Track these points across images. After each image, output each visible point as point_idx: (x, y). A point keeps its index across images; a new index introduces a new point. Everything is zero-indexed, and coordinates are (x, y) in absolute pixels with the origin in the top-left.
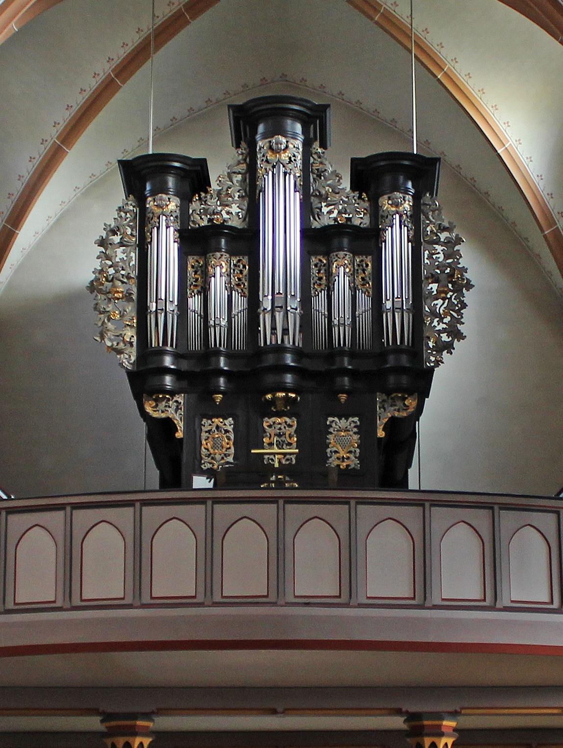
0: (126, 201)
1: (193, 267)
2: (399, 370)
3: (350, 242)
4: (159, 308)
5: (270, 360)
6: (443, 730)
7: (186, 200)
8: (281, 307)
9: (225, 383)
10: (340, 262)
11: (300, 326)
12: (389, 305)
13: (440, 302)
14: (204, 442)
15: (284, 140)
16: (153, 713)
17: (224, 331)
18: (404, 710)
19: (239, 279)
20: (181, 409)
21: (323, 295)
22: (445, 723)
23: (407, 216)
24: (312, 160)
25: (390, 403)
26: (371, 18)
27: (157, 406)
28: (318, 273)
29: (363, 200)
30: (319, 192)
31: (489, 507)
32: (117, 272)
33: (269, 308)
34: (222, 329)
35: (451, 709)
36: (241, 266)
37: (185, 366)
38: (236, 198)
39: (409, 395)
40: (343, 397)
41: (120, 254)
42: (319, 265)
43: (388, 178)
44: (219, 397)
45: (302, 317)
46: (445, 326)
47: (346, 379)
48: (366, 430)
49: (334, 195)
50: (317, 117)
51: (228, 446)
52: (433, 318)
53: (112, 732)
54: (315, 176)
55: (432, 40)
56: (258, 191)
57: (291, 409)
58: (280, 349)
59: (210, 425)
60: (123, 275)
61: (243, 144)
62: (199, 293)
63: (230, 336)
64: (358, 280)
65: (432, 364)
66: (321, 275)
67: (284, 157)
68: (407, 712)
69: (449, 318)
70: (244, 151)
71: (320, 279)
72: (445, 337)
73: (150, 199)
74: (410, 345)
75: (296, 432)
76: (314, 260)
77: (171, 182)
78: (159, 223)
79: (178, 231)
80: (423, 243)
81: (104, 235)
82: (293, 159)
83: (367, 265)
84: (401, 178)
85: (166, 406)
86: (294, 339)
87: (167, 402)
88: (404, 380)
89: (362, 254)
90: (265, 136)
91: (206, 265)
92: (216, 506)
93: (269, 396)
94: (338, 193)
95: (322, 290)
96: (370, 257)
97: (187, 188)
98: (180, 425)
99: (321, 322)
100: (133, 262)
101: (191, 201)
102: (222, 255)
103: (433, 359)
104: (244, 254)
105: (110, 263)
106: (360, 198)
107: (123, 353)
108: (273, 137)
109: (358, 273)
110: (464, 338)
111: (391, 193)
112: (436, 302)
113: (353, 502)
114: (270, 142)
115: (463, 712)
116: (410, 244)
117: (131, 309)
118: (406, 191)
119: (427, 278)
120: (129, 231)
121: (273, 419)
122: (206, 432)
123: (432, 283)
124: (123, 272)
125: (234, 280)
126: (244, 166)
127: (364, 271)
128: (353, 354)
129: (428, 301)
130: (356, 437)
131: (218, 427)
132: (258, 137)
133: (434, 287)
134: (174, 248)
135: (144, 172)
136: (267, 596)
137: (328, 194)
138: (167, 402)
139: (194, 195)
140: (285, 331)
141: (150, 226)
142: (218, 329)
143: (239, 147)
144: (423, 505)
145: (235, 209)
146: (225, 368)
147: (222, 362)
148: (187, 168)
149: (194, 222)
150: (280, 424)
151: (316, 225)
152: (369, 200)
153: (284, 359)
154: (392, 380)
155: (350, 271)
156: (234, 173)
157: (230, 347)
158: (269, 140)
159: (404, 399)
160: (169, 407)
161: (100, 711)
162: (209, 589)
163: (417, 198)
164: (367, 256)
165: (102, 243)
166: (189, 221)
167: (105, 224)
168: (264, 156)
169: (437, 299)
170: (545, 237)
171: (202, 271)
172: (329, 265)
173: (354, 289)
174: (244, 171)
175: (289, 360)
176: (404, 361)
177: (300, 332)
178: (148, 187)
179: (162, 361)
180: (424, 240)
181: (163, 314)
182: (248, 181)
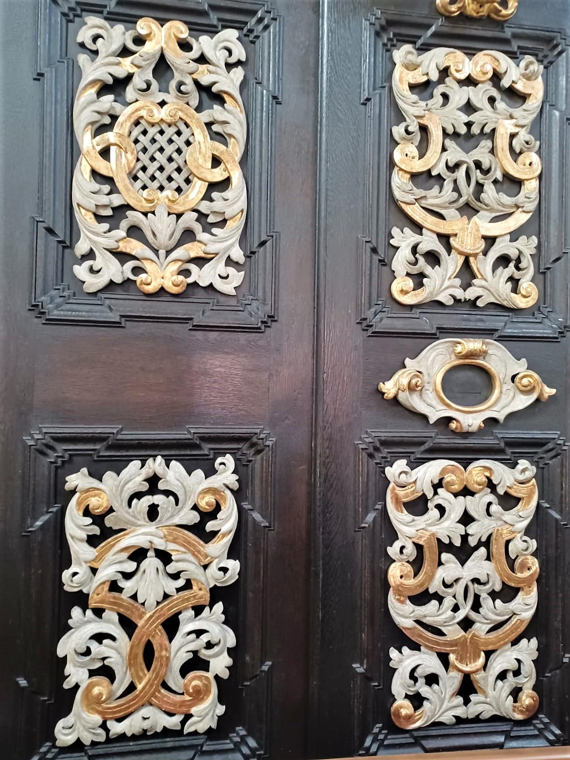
14: (88, 143)
51: (218, 175)
59: (125, 52)
75: (537, 127)
121: (438, 57)
122: (104, 89)
131: (162, 67)
150: (470, 81)
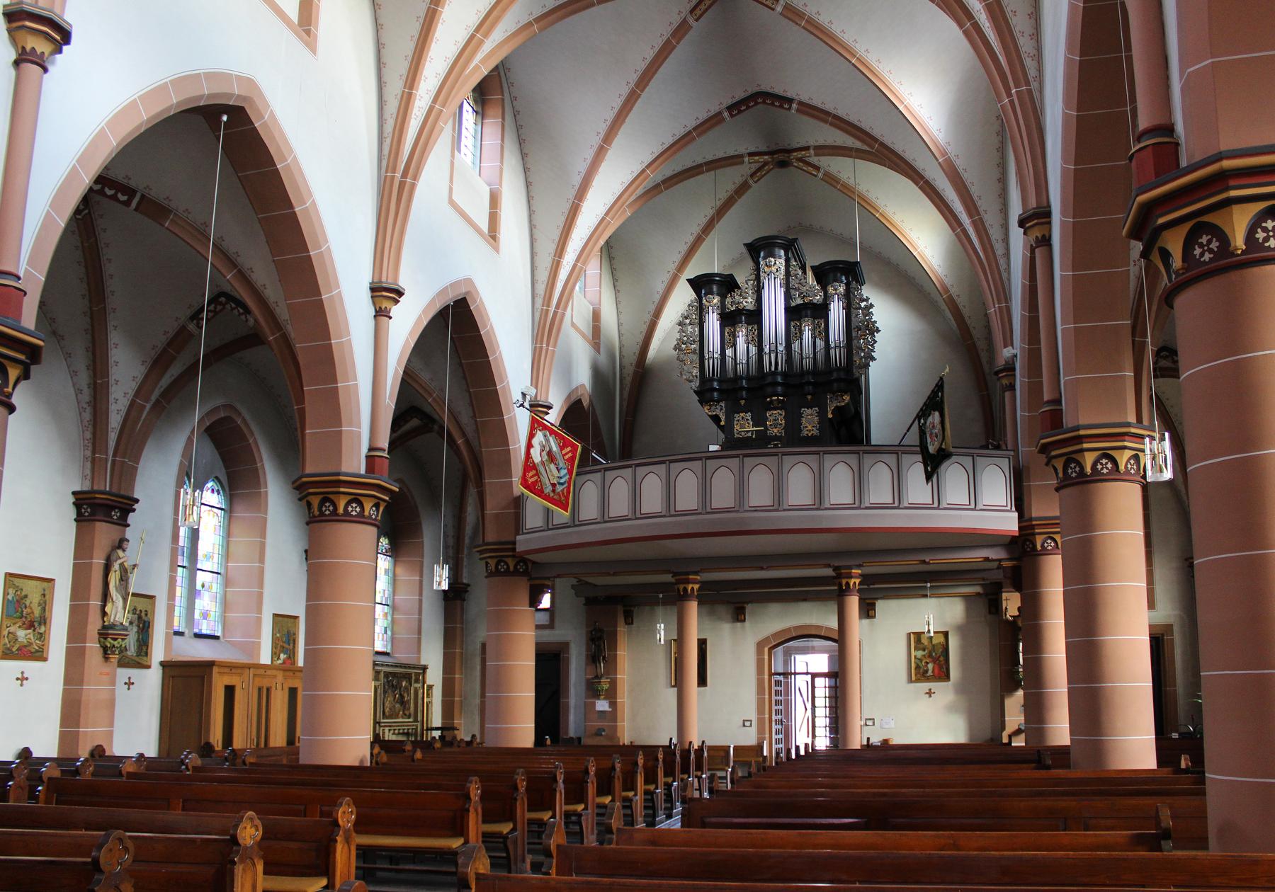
5: (769, 379)
7: (723, 297)
9: (746, 394)
15: (773, 260)
17: (745, 366)
21: (798, 342)
24: (791, 269)
37: (725, 386)
38: (750, 294)
40: (809, 397)
41: (690, 329)
44: (743, 402)
48: (822, 414)
53: (679, 582)
57: (782, 406)
58: (775, 373)
62: (732, 346)
64: (817, 333)
67: (774, 269)
76: (792, 324)
77: (715, 288)
81: (681, 319)
93: (768, 399)
98: (723, 418)
101: (726, 298)
117: (696, 357)
120: (694, 317)
125: (750, 338)
130: (817, 418)
134: (717, 324)
145: (750, 300)
148: (723, 280)
149: (728, 309)
151: (793, 304)
173: (814, 338)
175: (779, 379)
179: (712, 385)
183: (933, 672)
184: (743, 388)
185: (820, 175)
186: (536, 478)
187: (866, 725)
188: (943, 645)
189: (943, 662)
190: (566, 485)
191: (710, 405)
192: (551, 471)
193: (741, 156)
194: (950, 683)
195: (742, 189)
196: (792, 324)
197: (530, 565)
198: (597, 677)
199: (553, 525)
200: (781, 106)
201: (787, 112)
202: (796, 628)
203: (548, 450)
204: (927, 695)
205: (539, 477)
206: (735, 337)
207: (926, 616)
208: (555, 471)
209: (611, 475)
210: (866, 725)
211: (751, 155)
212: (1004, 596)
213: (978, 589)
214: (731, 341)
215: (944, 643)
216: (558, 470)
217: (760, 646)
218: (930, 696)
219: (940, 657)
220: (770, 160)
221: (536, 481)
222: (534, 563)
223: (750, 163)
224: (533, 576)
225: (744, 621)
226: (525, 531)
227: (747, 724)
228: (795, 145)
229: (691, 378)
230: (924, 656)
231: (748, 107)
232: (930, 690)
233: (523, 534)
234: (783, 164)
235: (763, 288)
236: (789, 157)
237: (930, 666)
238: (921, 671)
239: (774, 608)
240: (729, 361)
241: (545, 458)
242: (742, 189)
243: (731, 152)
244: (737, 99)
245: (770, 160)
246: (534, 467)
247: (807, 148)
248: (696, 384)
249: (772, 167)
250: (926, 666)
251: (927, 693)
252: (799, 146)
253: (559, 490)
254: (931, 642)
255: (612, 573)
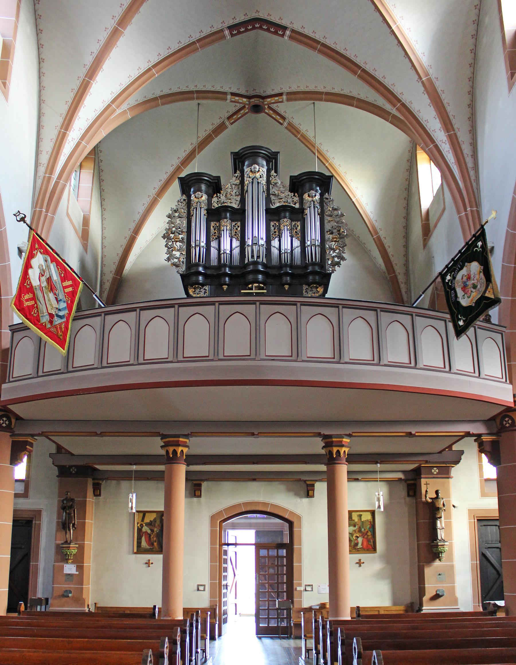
0: (181, 197)
1: (213, 227)
2: (314, 273)
3: (290, 215)
4: (196, 245)
5: (251, 267)
6: (343, 443)
7: (210, 197)
8: (257, 243)
10: (285, 224)
11: (266, 255)
12: (309, 243)
13: (334, 243)
15: (258, 167)
16: (188, 434)
17: (228, 256)
18: (322, 433)
19: (236, 232)
20: (207, 292)
21: (277, 240)
22: (344, 440)
23: (317, 202)
24: (271, 179)
25: (310, 290)
26: (296, 136)
27: (195, 291)
28: (274, 230)
29: (295, 196)
30: (274, 192)
31: (375, 309)
32: (176, 229)
33: (250, 244)
34: (228, 255)
35: (348, 433)
36: (237, 227)
37: (209, 272)
39: (320, 286)
41: (178, 221)
42: (274, 226)
43: (307, 186)
44: (225, 287)
45: (266, 249)
46: (336, 254)
47: (288, 278)
49: (282, 194)
50: (274, 158)
52: (330, 250)
54: (272, 186)
55: (324, 148)
56: (245, 192)
58: (256, 263)
60: (179, 231)
61: (238, 172)
62: (216, 239)
63: (231, 259)
65: (331, 272)
66: (275, 231)
67: (258, 175)
68: (324, 434)
69: (337, 251)
70: (238, 175)
71: (275, 232)
72: (336, 259)
73: (193, 195)
74: (320, 262)
76: (272, 223)
78: (197, 205)
79: (207, 210)
80: (325, 216)
81: (171, 212)
82: (262, 176)
83: (298, 226)
84: (314, 185)
85: (199, 291)
86: (263, 259)
87: (200, 290)
88: (317, 278)
89: (296, 221)
90: (249, 166)
91: (220, 225)
92: (221, 306)
94: (284, 193)
95: (276, 237)
96: (299, 222)
97: (211, 191)
99: (275, 252)
100: (185, 225)
101: (213, 197)
102: (228, 221)
103: (331, 269)
104: (238, 221)
105: (173, 225)
106: (294, 196)
107: (179, 267)
108: (252, 166)
109: (293, 230)
110: (345, 260)
111: (309, 192)
112: (331, 243)
113: (299, 304)
114: (251, 168)
115: (354, 434)
116: (319, 216)
118: (317, 191)
119: (327, 232)
120: (183, 211)
123: (330, 234)
124: (179, 230)
125: (233, 234)
126: (238, 181)
127: (296, 228)
128: (291, 266)
129: (328, 243)
132: (245, 167)
133: (331, 236)
135: (191, 182)
136: (250, 356)
137: (279, 194)
138: (200, 290)
139: (214, 194)
140: (258, 257)
141: (193, 208)
142: (225, 255)
143: (236, 173)
144: (338, 307)
146: (229, 272)
147: (227, 270)
149: (214, 206)
152: (298, 197)
153: (257, 267)
154: (311, 278)
155: (290, 228)
156: (234, 184)
157: (231, 263)
158: (251, 167)
159: (317, 288)
160: (201, 292)
161: (161, 433)
162: (216, 352)
163: (321, 195)
164: (298, 221)
165: (169, 216)
166: (212, 206)
167: (171, 208)
168: (248, 175)
169: (332, 242)
170: (374, 239)
171: (218, 229)
172: (279, 226)
174: (238, 184)
175: (260, 268)
176: (317, 269)
177: (265, 257)
178: (192, 190)
179: (198, 269)
180: (326, 215)
181: (198, 248)
182: (240, 188)
183: (362, 544)
184: (226, 274)
185: (285, 124)
186: (33, 302)
187: (306, 590)
188: (370, 522)
189: (370, 537)
190: (64, 320)
191: (194, 288)
192: (49, 300)
193: (225, 93)
194: (376, 554)
195: (220, 128)
196: (272, 223)
197: (13, 421)
198: (66, 542)
199: (43, 372)
200: (276, 33)
201: (279, 38)
202: (245, 504)
203: (48, 276)
204: (358, 565)
205: (36, 303)
206: (219, 230)
207: (377, 494)
208: (54, 302)
209: (111, 319)
210: (306, 590)
211: (233, 94)
212: (423, 481)
213: (401, 476)
214: (217, 234)
215: (372, 521)
216: (58, 301)
217: (213, 518)
218: (360, 566)
219: (368, 532)
220: (247, 102)
221: (33, 305)
222: (18, 418)
223: (231, 101)
224: (16, 432)
225: (200, 496)
226: (11, 379)
227: (201, 588)
228: (269, 92)
229: (178, 263)
230: (355, 531)
231: (247, 30)
232: (360, 560)
233: (10, 382)
234: (257, 109)
235: (247, 191)
236: (263, 102)
237: (360, 540)
238: (353, 544)
239: (227, 485)
240: (214, 252)
241: (44, 284)
242: (220, 128)
243: (218, 89)
244: (237, 21)
245: (247, 102)
246: (31, 290)
247: (281, 94)
248: (183, 269)
249: (247, 111)
250: (357, 539)
251: (357, 563)
252: (273, 93)
253: (57, 323)
254: (361, 519)
255: (99, 433)
